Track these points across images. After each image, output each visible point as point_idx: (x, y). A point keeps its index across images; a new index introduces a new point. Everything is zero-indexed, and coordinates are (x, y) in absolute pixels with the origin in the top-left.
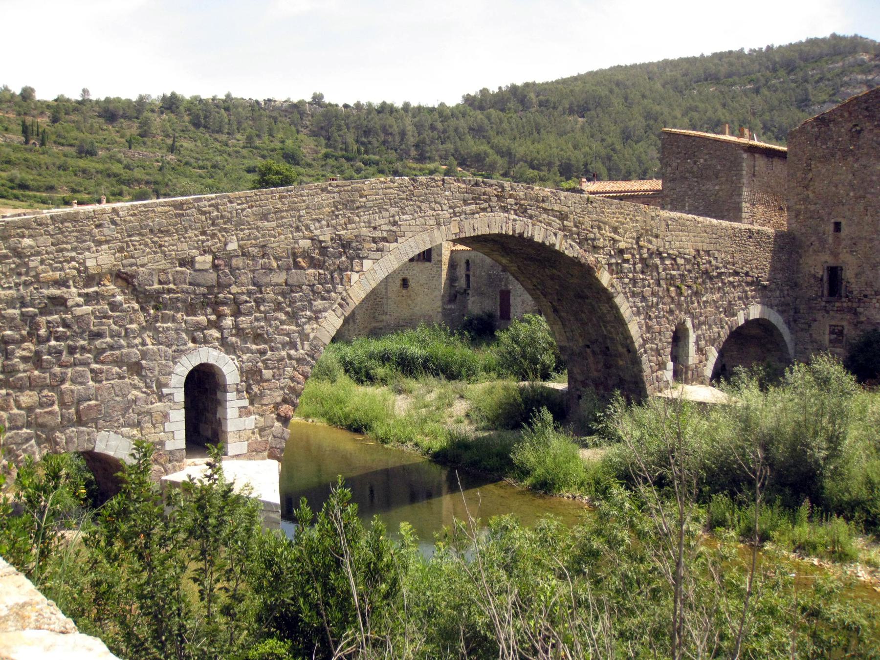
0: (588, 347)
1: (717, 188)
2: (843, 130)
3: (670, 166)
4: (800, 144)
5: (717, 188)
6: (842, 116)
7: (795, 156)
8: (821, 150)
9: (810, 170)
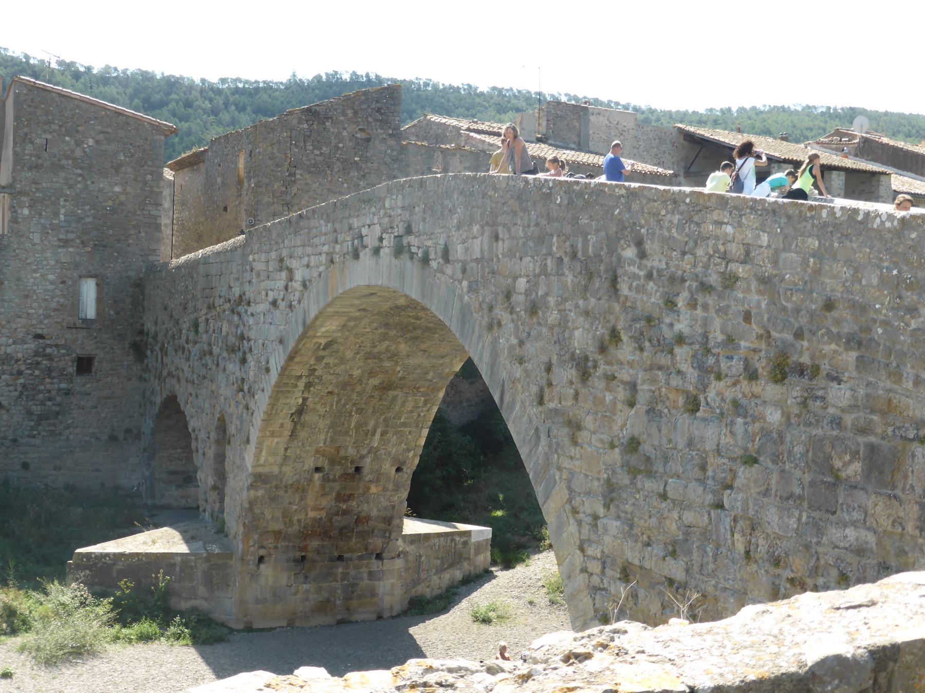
0: (318, 470)
1: (117, 189)
2: (345, 133)
3: (32, 142)
4: (279, 142)
5: (117, 189)
6: (344, 114)
7: (270, 158)
8: (312, 156)
9: (294, 182)
